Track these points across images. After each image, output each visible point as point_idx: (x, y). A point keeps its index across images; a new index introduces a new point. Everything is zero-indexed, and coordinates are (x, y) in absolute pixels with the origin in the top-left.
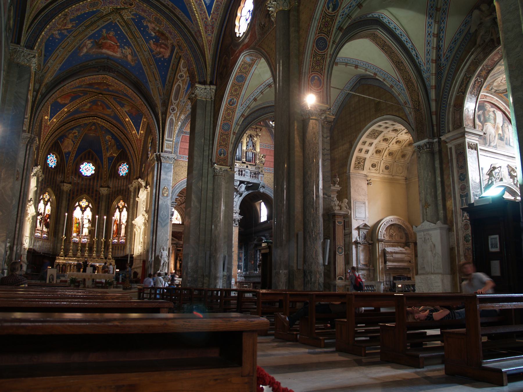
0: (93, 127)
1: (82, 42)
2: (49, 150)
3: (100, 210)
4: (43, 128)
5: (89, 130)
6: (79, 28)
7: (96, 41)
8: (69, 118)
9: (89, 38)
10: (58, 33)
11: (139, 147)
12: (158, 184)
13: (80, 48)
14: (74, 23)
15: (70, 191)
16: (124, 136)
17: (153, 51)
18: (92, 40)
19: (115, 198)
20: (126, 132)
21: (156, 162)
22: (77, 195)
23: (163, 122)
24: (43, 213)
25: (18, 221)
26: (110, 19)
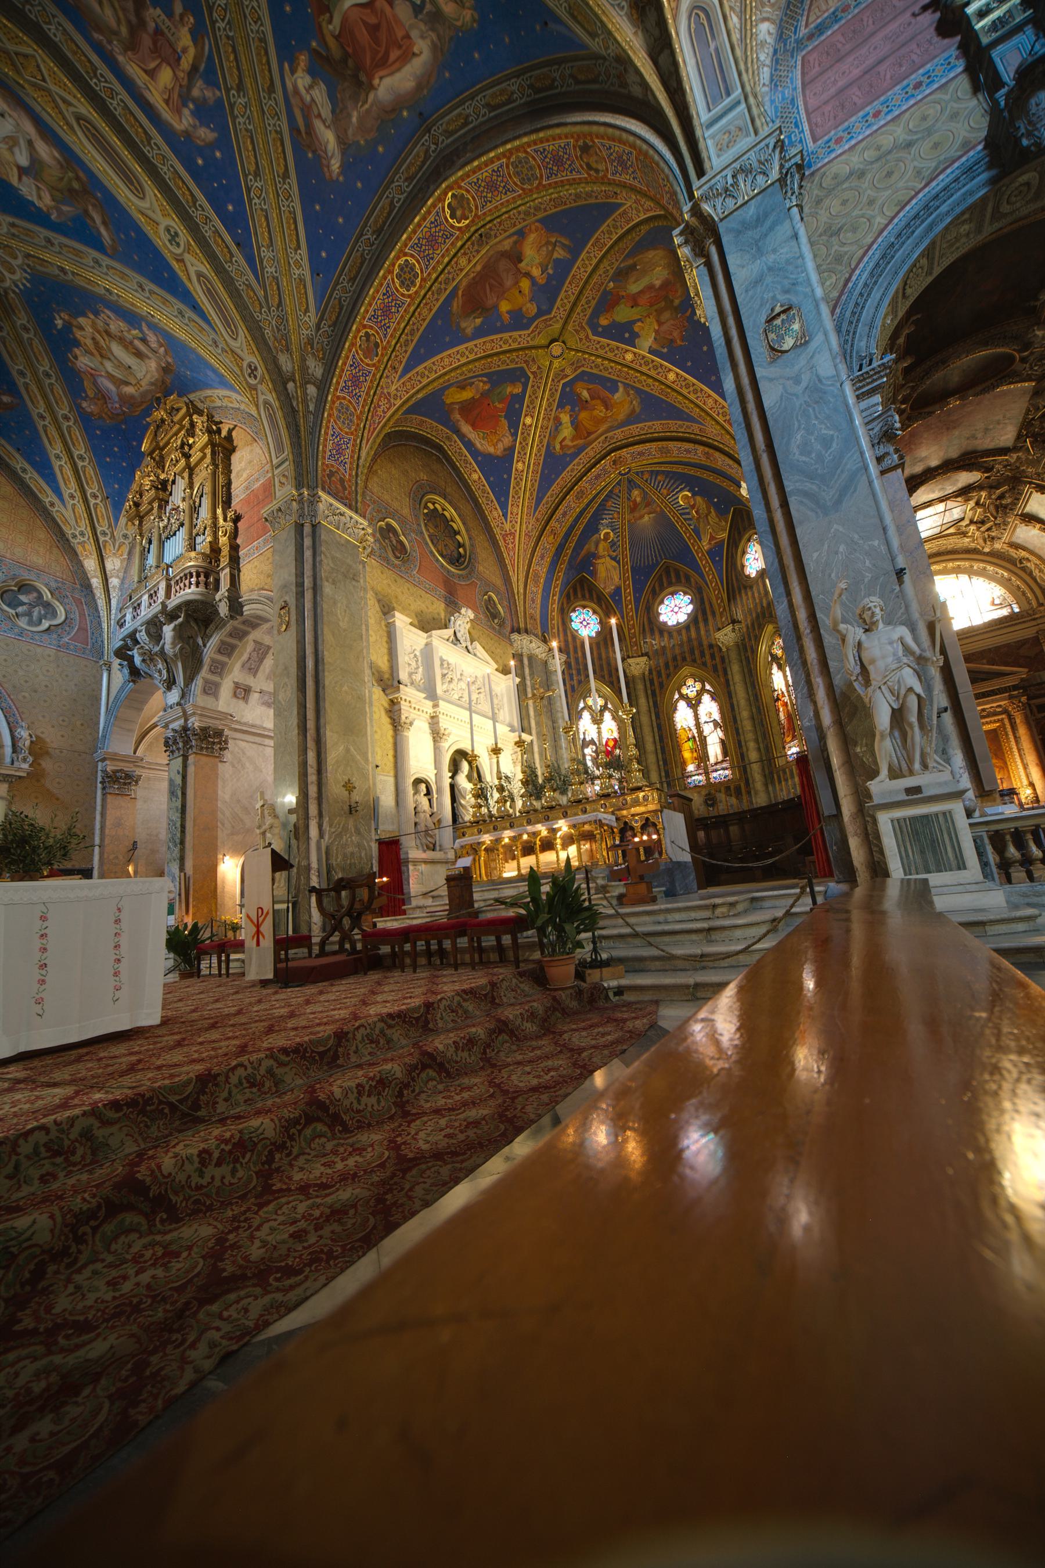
4: (501, 543)
7: (315, 51)
9: (287, 55)
15: (650, 671)
16: (700, 448)
20: (695, 428)
24: (596, 740)
25: (311, 744)
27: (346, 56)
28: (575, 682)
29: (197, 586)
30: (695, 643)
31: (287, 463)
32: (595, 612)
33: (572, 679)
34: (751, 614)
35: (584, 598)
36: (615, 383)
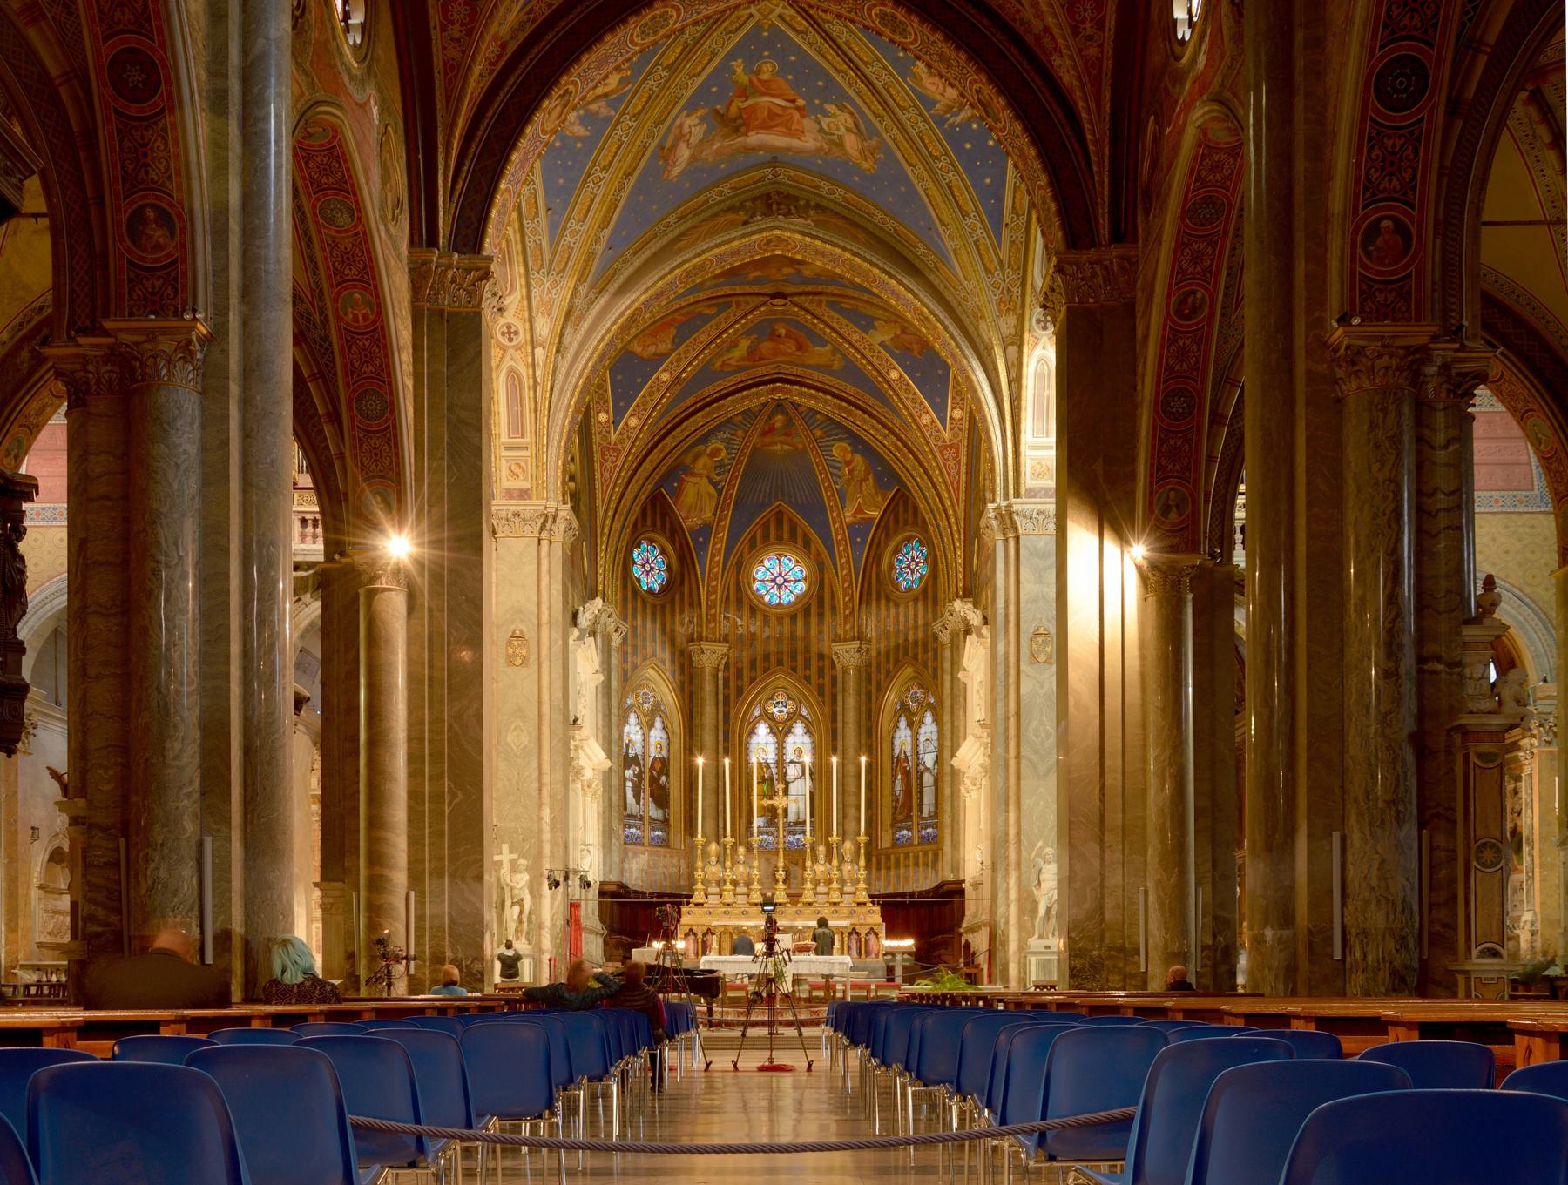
0: (779, 420)
1: (670, 128)
2: (633, 532)
3: (840, 725)
4: (597, 457)
5: (764, 433)
6: (645, 79)
7: (717, 112)
8: (683, 405)
9: (691, 107)
10: (579, 117)
11: (954, 472)
12: (1012, 618)
13: (665, 153)
17: (935, 102)
18: (702, 112)
19: (890, 676)
20: (898, 422)
21: (999, 537)
22: (752, 680)
23: (1013, 375)
26: (751, 15)
27: (740, 116)
28: (629, 666)
30: (800, 645)
31: (527, 453)
32: (663, 552)
33: (625, 661)
34: (888, 638)
35: (654, 529)
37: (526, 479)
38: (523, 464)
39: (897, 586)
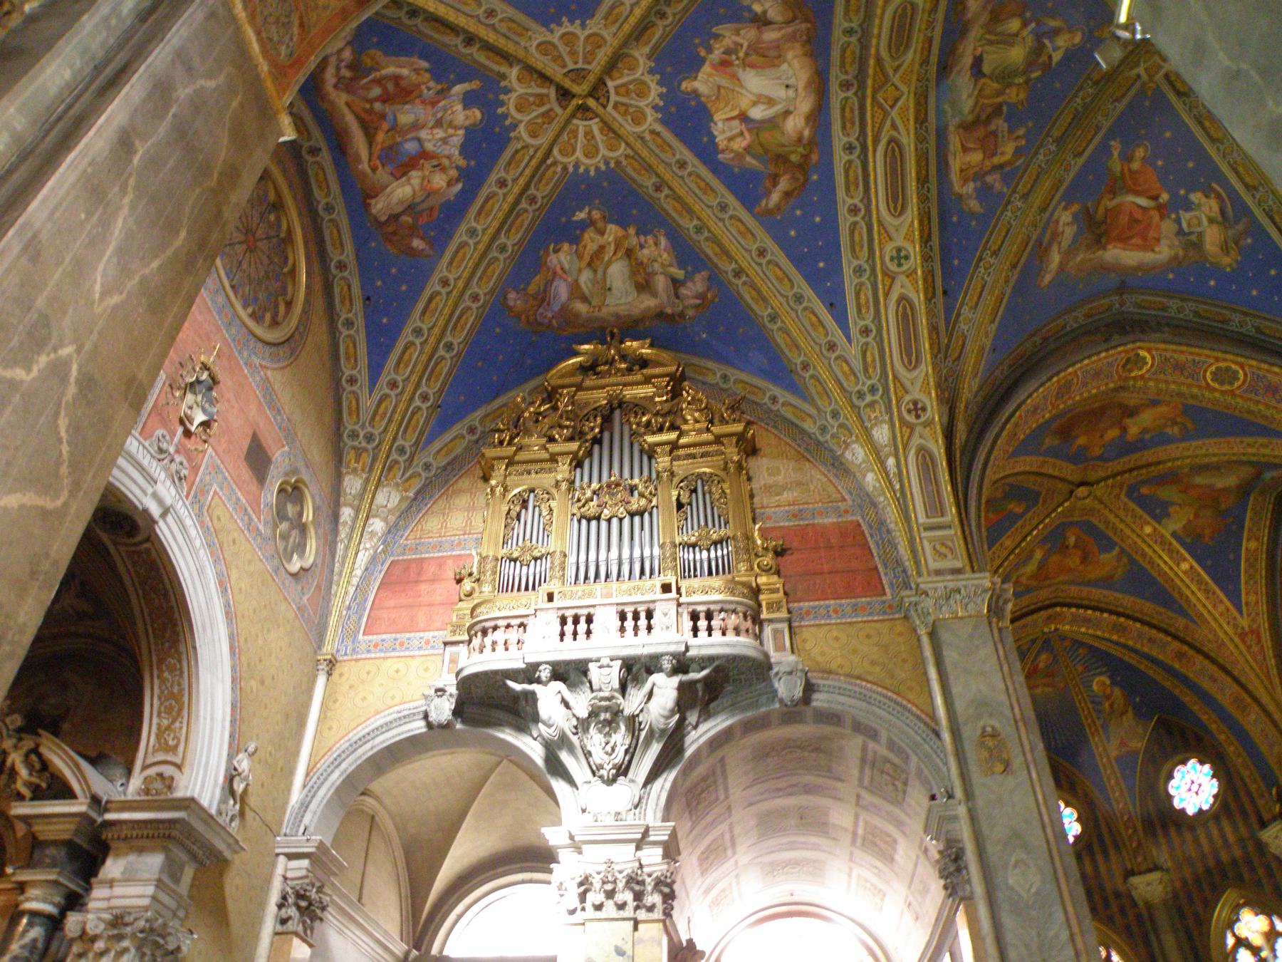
1: (1048, 222)
6: (1036, 153)
9: (1068, 199)
10: (975, 189)
13: (1041, 250)
14: (1021, 132)
18: (1076, 208)
20: (1180, 623)
27: (1104, 222)
29: (724, 634)
36: (1112, 545)
37: (956, 558)
38: (950, 544)
39: (1183, 811)
